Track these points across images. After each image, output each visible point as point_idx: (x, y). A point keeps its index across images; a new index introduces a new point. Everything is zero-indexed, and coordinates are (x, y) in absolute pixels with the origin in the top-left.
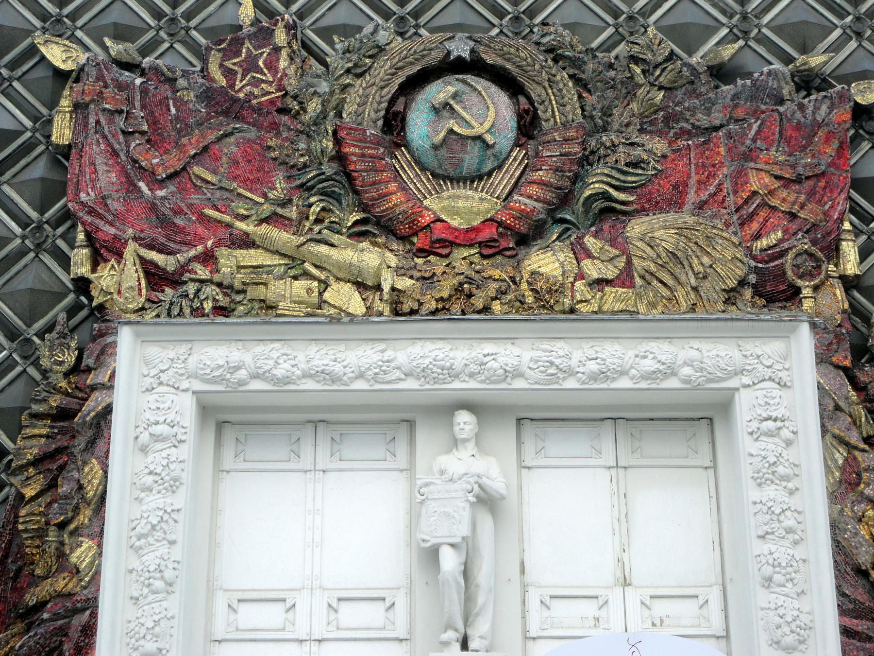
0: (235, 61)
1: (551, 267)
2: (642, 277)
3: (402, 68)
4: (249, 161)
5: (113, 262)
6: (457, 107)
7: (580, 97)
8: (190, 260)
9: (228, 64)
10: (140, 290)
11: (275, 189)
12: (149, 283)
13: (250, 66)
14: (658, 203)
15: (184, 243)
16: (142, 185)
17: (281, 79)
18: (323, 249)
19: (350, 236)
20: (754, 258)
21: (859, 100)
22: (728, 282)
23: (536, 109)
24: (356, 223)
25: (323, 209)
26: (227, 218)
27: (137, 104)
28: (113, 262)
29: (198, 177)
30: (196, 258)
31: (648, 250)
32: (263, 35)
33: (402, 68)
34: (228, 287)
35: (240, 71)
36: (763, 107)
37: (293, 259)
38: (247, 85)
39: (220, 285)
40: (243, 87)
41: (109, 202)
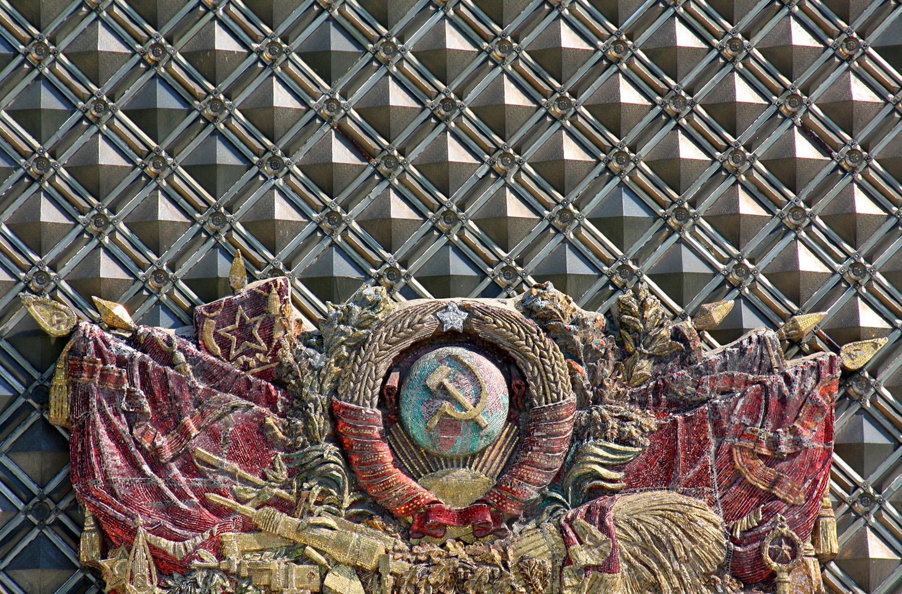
0: (229, 328)
1: (541, 550)
2: (628, 561)
3: (396, 343)
4: (248, 441)
5: (123, 548)
6: (451, 387)
7: (570, 367)
8: (196, 548)
9: (221, 331)
10: (151, 576)
11: (274, 469)
12: (157, 567)
13: (245, 332)
14: (645, 479)
15: (192, 529)
16: (146, 468)
17: (276, 349)
18: (325, 532)
19: (349, 518)
20: (733, 539)
21: (848, 364)
22: (708, 565)
23: (527, 385)
24: (353, 505)
25: (322, 492)
26: (230, 502)
27: (137, 381)
28: (123, 548)
29: (199, 460)
30: (203, 545)
31: (632, 533)
32: (258, 302)
33: (396, 343)
34: (234, 574)
35: (235, 338)
36: (751, 377)
37: (295, 543)
38: (242, 354)
39: (226, 572)
40: (238, 356)
41: (116, 486)
